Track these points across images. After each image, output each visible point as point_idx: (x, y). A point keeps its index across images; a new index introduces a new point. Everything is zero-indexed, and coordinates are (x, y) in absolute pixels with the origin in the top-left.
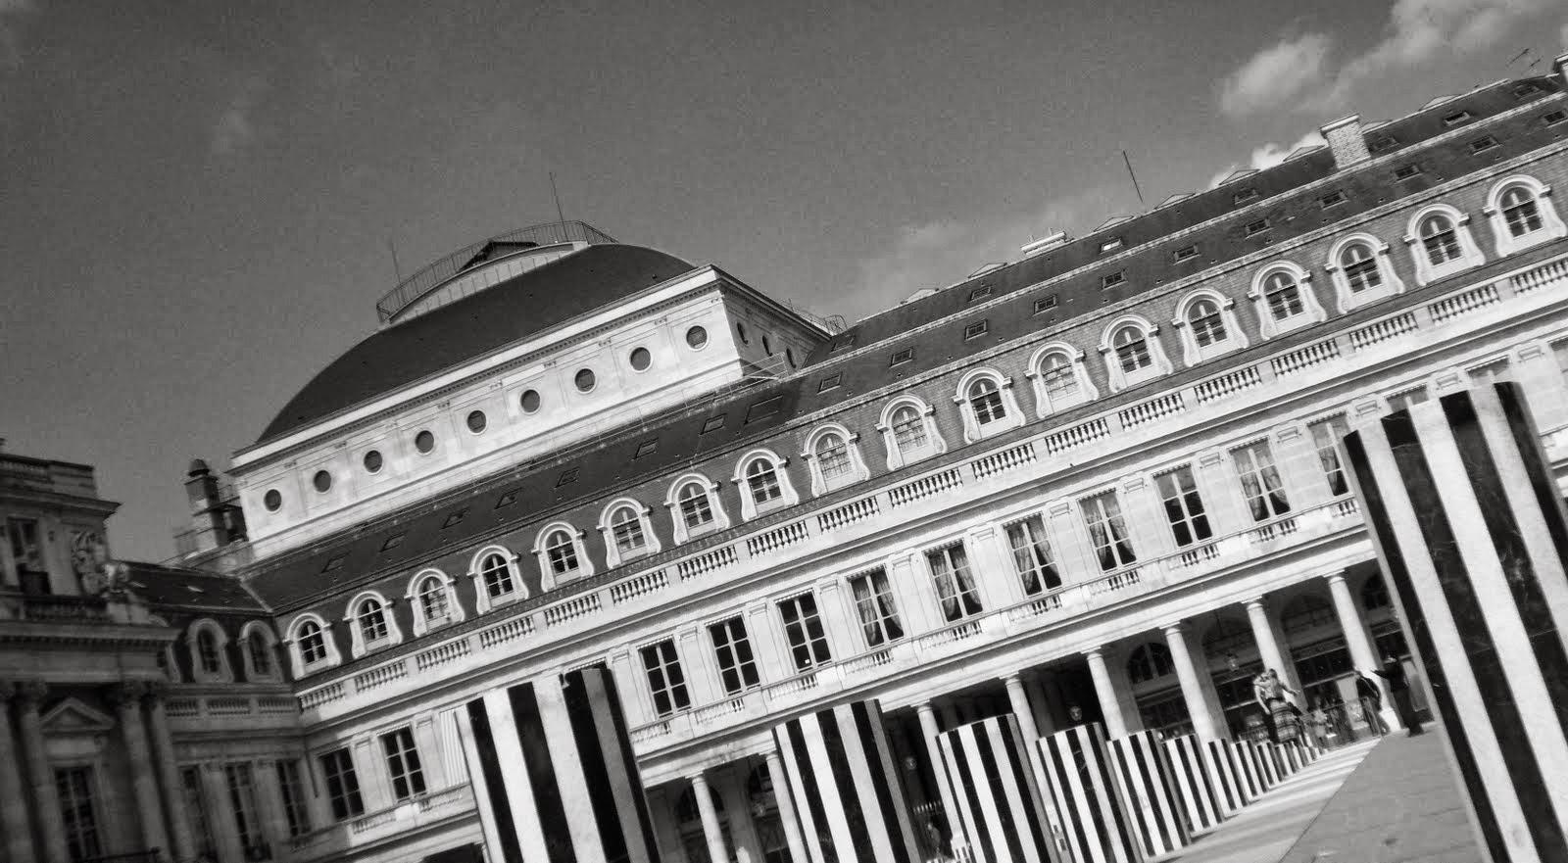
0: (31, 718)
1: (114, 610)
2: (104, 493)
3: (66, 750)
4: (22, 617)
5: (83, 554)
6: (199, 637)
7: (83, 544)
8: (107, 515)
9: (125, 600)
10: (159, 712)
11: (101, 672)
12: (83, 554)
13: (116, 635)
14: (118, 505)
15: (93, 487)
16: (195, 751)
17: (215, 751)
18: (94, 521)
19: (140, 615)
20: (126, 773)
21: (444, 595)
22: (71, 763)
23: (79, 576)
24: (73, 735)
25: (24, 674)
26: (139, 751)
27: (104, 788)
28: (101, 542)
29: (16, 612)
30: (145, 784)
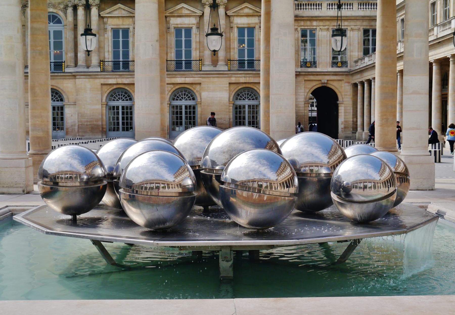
16: (315, 23)
17: (328, 23)
24: (247, 16)
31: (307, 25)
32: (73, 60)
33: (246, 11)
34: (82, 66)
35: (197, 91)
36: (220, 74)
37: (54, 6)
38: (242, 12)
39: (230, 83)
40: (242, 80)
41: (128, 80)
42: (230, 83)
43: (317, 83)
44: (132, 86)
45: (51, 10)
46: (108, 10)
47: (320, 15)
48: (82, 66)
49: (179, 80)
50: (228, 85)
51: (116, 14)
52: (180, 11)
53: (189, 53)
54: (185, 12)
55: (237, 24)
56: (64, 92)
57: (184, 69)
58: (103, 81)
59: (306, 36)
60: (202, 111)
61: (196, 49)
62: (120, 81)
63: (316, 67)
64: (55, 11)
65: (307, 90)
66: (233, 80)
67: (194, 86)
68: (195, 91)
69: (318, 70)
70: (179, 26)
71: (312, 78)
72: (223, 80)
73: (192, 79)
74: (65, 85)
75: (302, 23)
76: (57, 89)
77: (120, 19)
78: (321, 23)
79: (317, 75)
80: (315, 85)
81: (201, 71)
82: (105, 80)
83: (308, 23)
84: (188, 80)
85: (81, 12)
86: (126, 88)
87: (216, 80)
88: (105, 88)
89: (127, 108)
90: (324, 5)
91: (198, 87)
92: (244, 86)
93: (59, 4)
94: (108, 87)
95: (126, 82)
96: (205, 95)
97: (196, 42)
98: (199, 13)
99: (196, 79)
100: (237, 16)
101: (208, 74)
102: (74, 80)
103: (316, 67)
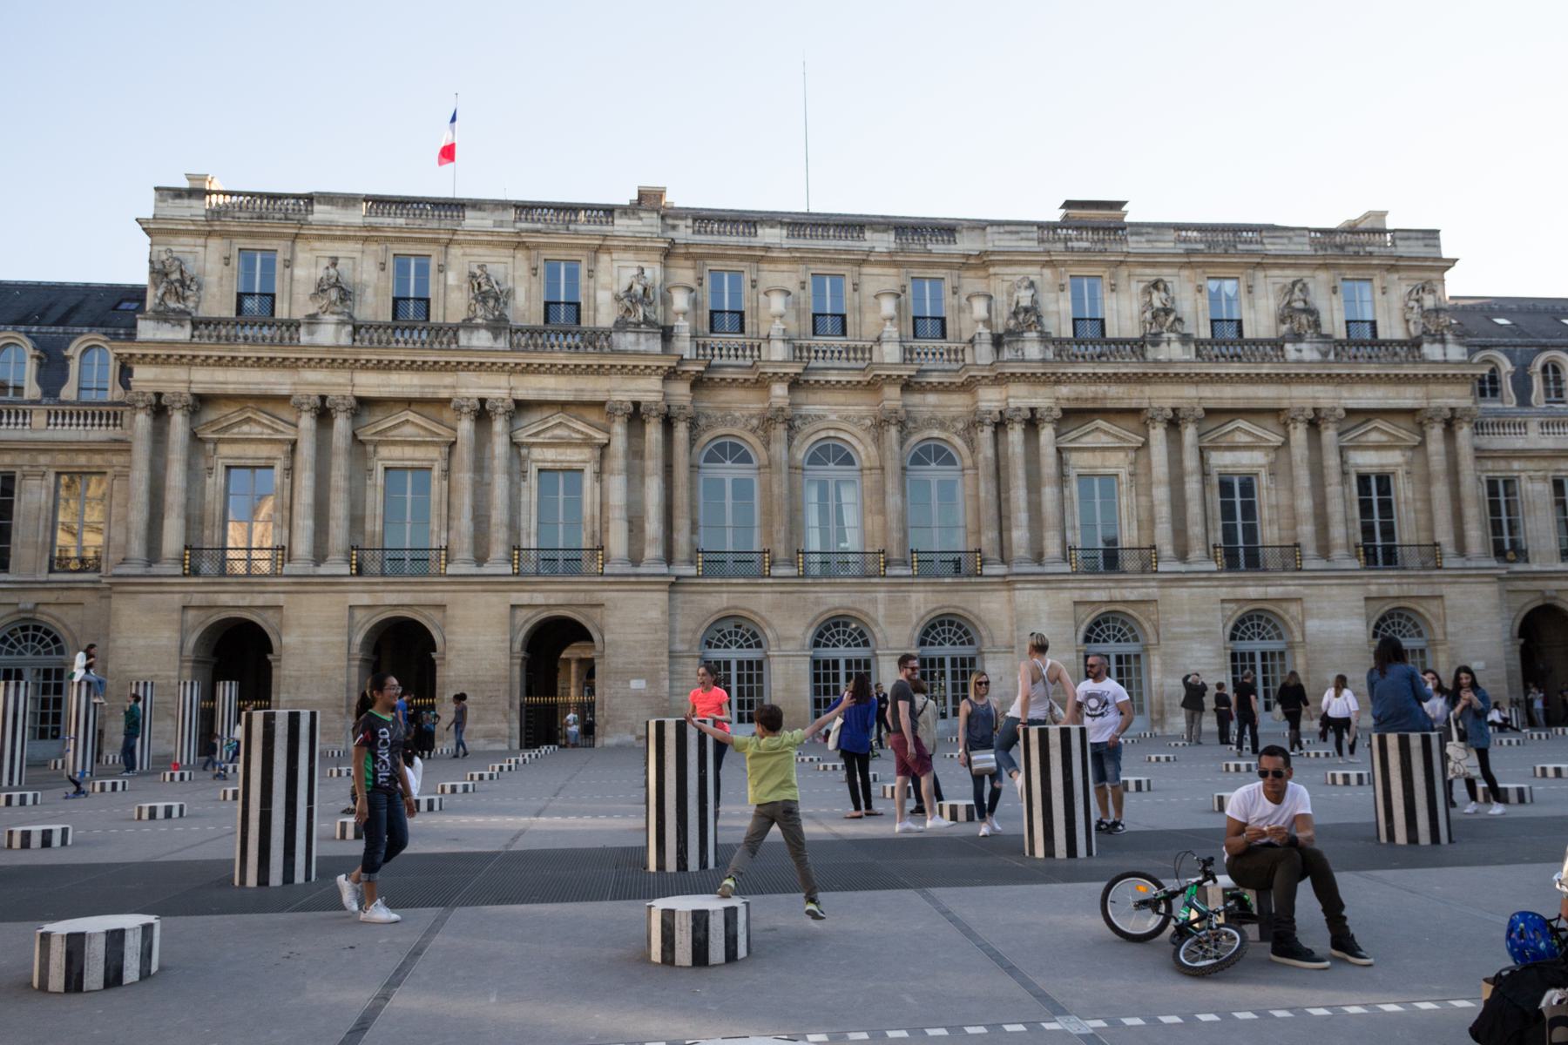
0: (1329, 435)
1: (1432, 351)
2: (1446, 253)
3: (1366, 460)
4: (1332, 357)
5: (1412, 303)
6: (1545, 369)
7: (1414, 295)
8: (1448, 268)
9: (1443, 341)
10: (1464, 433)
11: (1408, 397)
12: (1412, 303)
13: (1421, 370)
14: (1455, 261)
15: (1438, 246)
16: (1516, 465)
17: (1544, 464)
18: (1434, 275)
19: (1455, 352)
20: (1428, 480)
21: (1174, 410)
22: (1376, 470)
23: (1407, 321)
24: (1379, 447)
25: (1325, 403)
26: (1438, 461)
27: (1403, 491)
28: (1433, 292)
29: (1325, 354)
30: (1440, 490)
31: (1498, 469)
32: (997, 548)
33: (1374, 437)
34: (1021, 561)
35: (1293, 618)
36: (1343, 576)
37: (942, 425)
38: (1364, 439)
39: (1367, 599)
40: (1394, 591)
41: (1136, 592)
42: (1367, 599)
43: (1532, 596)
44: (1142, 607)
45: (936, 433)
46: (1073, 434)
47: (1527, 446)
48: (1021, 561)
49: (1252, 592)
50: (1362, 603)
51: (1088, 441)
52: (1228, 438)
53: (1251, 532)
54: (1241, 438)
55: (1357, 465)
56: (983, 623)
57: (1242, 566)
58: (1077, 595)
59: (1497, 494)
60: (1308, 664)
61: (1271, 522)
62: (1117, 594)
63: (1527, 561)
64: (943, 435)
65: (1513, 614)
66: (1374, 590)
67: (1285, 605)
68: (1287, 617)
69: (1535, 567)
70: (1230, 470)
71: (1521, 585)
72: (1351, 590)
73: (1281, 589)
74: (983, 605)
75: (1489, 464)
76: (826, 616)
77: (1098, 454)
78: (1531, 465)
79: (1535, 579)
80: (1530, 602)
81: (1300, 570)
82: (1083, 592)
83: (1502, 464)
84: (1273, 592)
85: (1016, 435)
86: (1130, 611)
87: (1335, 591)
88: (1081, 609)
89: (858, 663)
90: (1533, 426)
91: (1294, 609)
92: (1395, 604)
93: (954, 419)
94: (1088, 609)
95: (1132, 598)
96: (1312, 625)
97: (1270, 507)
98: (1276, 440)
99: (1292, 589)
100: (1356, 448)
101: (1317, 576)
102: (1005, 594)
103: (1527, 561)
